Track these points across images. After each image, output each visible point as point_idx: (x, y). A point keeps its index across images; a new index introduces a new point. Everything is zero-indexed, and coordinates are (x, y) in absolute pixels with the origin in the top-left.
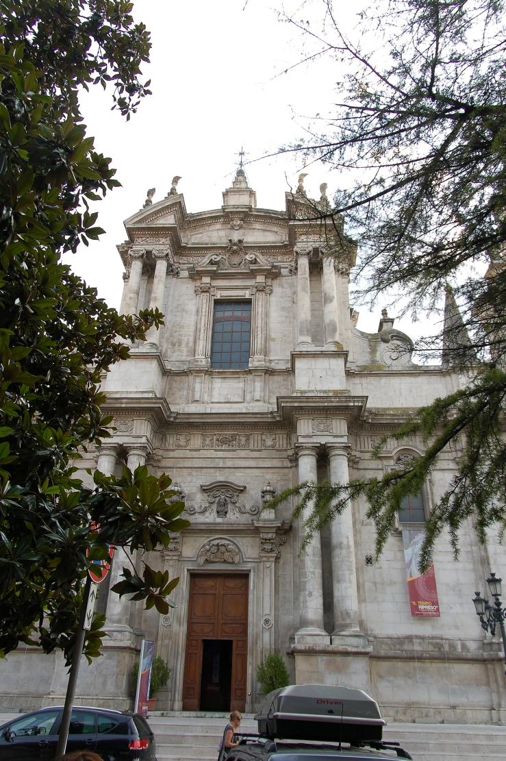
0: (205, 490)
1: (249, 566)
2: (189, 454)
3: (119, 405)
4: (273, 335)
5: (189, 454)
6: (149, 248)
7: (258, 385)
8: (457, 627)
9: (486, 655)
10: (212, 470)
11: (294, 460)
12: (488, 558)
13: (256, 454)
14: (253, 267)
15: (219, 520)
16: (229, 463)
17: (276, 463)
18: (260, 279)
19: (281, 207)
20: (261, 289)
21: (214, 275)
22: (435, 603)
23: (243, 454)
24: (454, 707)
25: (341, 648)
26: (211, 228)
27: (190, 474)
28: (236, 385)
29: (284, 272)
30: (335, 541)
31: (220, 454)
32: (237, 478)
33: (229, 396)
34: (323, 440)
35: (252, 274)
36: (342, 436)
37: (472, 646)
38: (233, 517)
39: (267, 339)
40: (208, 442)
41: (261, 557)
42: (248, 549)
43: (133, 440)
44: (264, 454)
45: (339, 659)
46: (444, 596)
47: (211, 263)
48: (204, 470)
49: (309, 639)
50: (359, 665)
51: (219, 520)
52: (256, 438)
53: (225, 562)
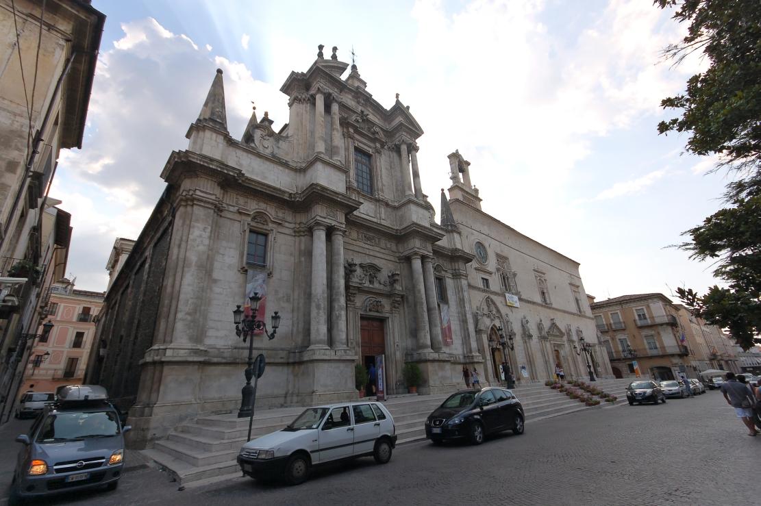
0: (361, 266)
1: (387, 315)
2: (351, 241)
3: (336, 198)
4: (384, 183)
5: (351, 241)
6: (331, 91)
7: (383, 210)
8: (456, 349)
9: (468, 361)
10: (364, 255)
11: (408, 260)
12: (466, 319)
13: (383, 251)
14: (377, 136)
15: (371, 286)
16: (371, 253)
17: (392, 259)
18: (378, 145)
19: (388, 104)
20: (379, 153)
21: (356, 130)
22: (451, 339)
23: (378, 249)
24: (458, 384)
25: (443, 359)
26: (347, 95)
27: (353, 255)
28: (371, 206)
29: (386, 147)
30: (432, 306)
31: (367, 246)
32: (376, 262)
33: (368, 211)
34: (426, 253)
35: (374, 140)
36: (430, 252)
37: (461, 357)
38: (376, 285)
39: (383, 185)
40: (360, 237)
41: (392, 310)
42: (386, 304)
43: (338, 224)
44: (387, 252)
45: (442, 364)
46: (453, 337)
47: (358, 121)
48: (360, 254)
49: (431, 354)
50: (448, 366)
51: (371, 286)
52: (383, 242)
53: (377, 311)
